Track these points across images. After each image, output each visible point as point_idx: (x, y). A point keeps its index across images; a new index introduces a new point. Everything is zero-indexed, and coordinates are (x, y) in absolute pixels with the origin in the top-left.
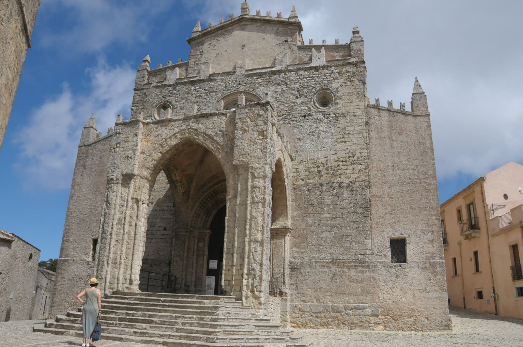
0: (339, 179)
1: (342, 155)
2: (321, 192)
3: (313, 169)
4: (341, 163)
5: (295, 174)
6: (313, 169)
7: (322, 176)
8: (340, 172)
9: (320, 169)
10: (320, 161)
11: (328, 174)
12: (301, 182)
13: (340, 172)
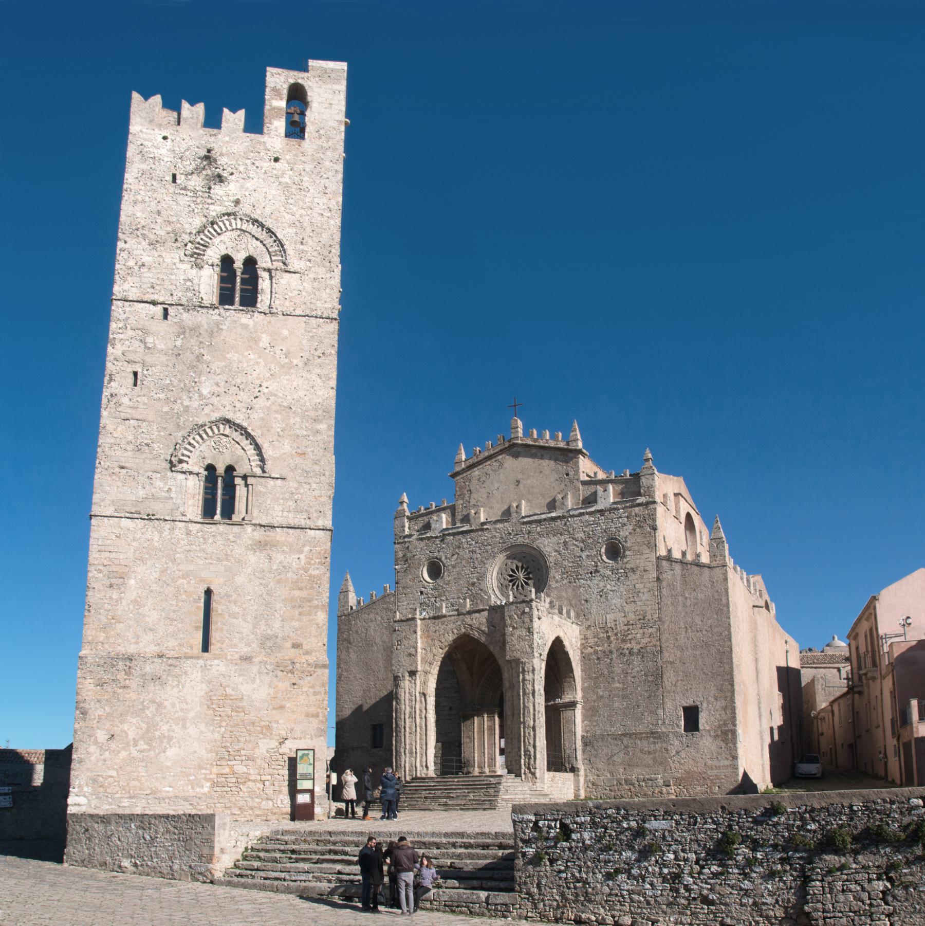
0: (629, 645)
1: (632, 617)
2: (611, 660)
3: (602, 635)
4: (631, 627)
5: (583, 642)
6: (602, 635)
7: (611, 642)
8: (630, 637)
9: (610, 634)
10: (609, 625)
11: (617, 639)
12: (590, 650)
13: (630, 637)
